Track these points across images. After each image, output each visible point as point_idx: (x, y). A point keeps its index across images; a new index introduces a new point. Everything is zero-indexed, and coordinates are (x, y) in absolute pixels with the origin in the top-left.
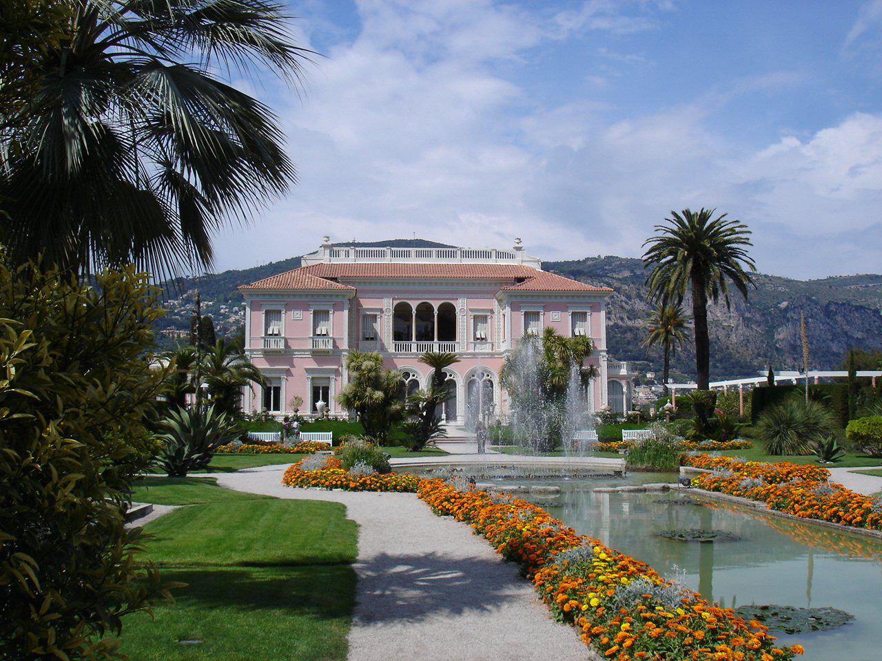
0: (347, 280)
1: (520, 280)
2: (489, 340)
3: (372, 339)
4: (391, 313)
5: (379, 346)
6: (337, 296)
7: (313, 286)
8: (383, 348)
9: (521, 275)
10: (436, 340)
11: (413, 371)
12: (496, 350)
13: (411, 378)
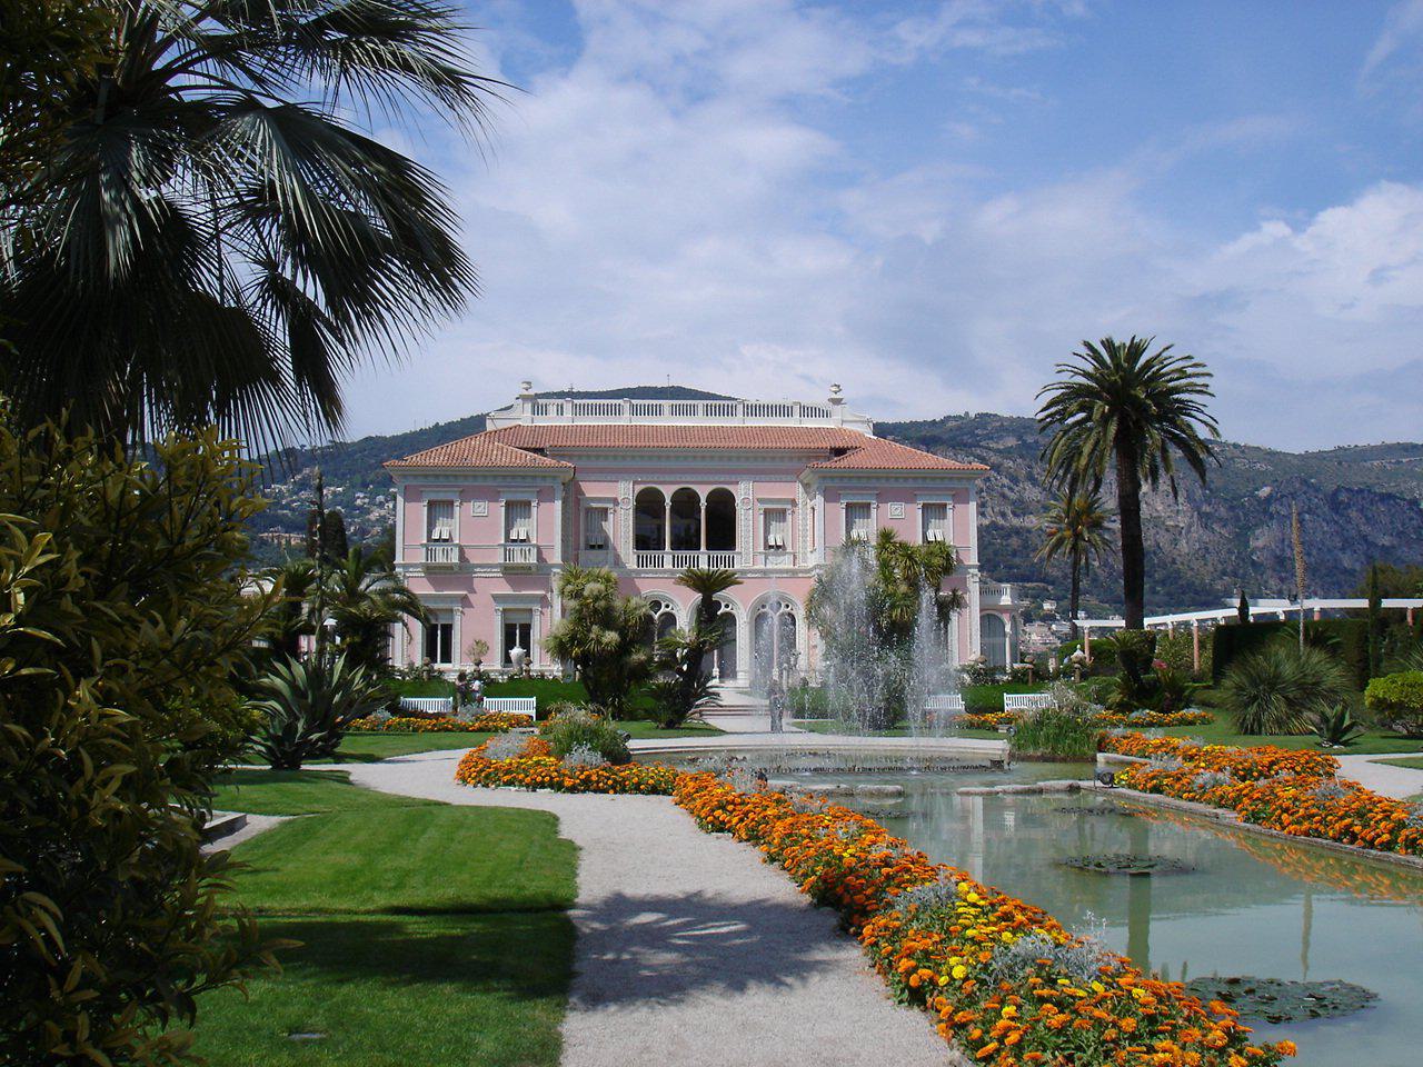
0: (559, 452)
1: (839, 452)
2: (789, 550)
3: (600, 547)
4: (631, 505)
5: (611, 558)
6: (544, 478)
7: (505, 461)
8: (617, 562)
9: (840, 444)
10: (703, 548)
11: (666, 599)
12: (801, 565)
13: (663, 610)
